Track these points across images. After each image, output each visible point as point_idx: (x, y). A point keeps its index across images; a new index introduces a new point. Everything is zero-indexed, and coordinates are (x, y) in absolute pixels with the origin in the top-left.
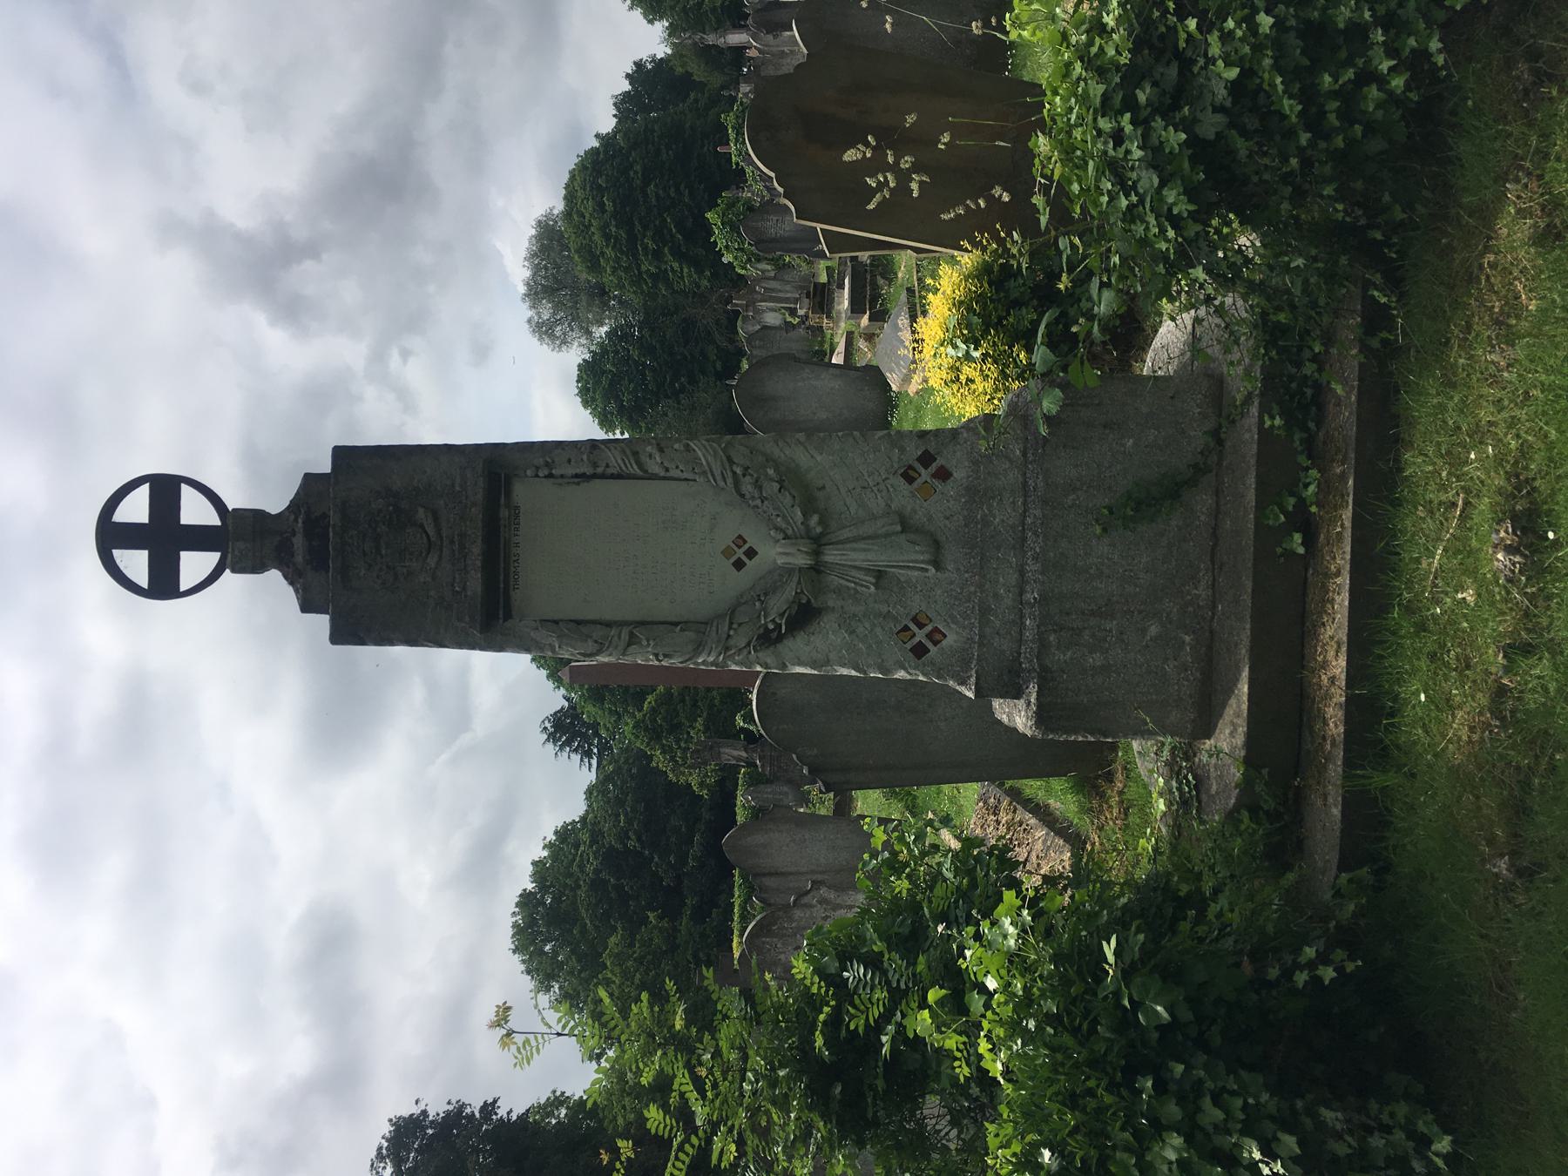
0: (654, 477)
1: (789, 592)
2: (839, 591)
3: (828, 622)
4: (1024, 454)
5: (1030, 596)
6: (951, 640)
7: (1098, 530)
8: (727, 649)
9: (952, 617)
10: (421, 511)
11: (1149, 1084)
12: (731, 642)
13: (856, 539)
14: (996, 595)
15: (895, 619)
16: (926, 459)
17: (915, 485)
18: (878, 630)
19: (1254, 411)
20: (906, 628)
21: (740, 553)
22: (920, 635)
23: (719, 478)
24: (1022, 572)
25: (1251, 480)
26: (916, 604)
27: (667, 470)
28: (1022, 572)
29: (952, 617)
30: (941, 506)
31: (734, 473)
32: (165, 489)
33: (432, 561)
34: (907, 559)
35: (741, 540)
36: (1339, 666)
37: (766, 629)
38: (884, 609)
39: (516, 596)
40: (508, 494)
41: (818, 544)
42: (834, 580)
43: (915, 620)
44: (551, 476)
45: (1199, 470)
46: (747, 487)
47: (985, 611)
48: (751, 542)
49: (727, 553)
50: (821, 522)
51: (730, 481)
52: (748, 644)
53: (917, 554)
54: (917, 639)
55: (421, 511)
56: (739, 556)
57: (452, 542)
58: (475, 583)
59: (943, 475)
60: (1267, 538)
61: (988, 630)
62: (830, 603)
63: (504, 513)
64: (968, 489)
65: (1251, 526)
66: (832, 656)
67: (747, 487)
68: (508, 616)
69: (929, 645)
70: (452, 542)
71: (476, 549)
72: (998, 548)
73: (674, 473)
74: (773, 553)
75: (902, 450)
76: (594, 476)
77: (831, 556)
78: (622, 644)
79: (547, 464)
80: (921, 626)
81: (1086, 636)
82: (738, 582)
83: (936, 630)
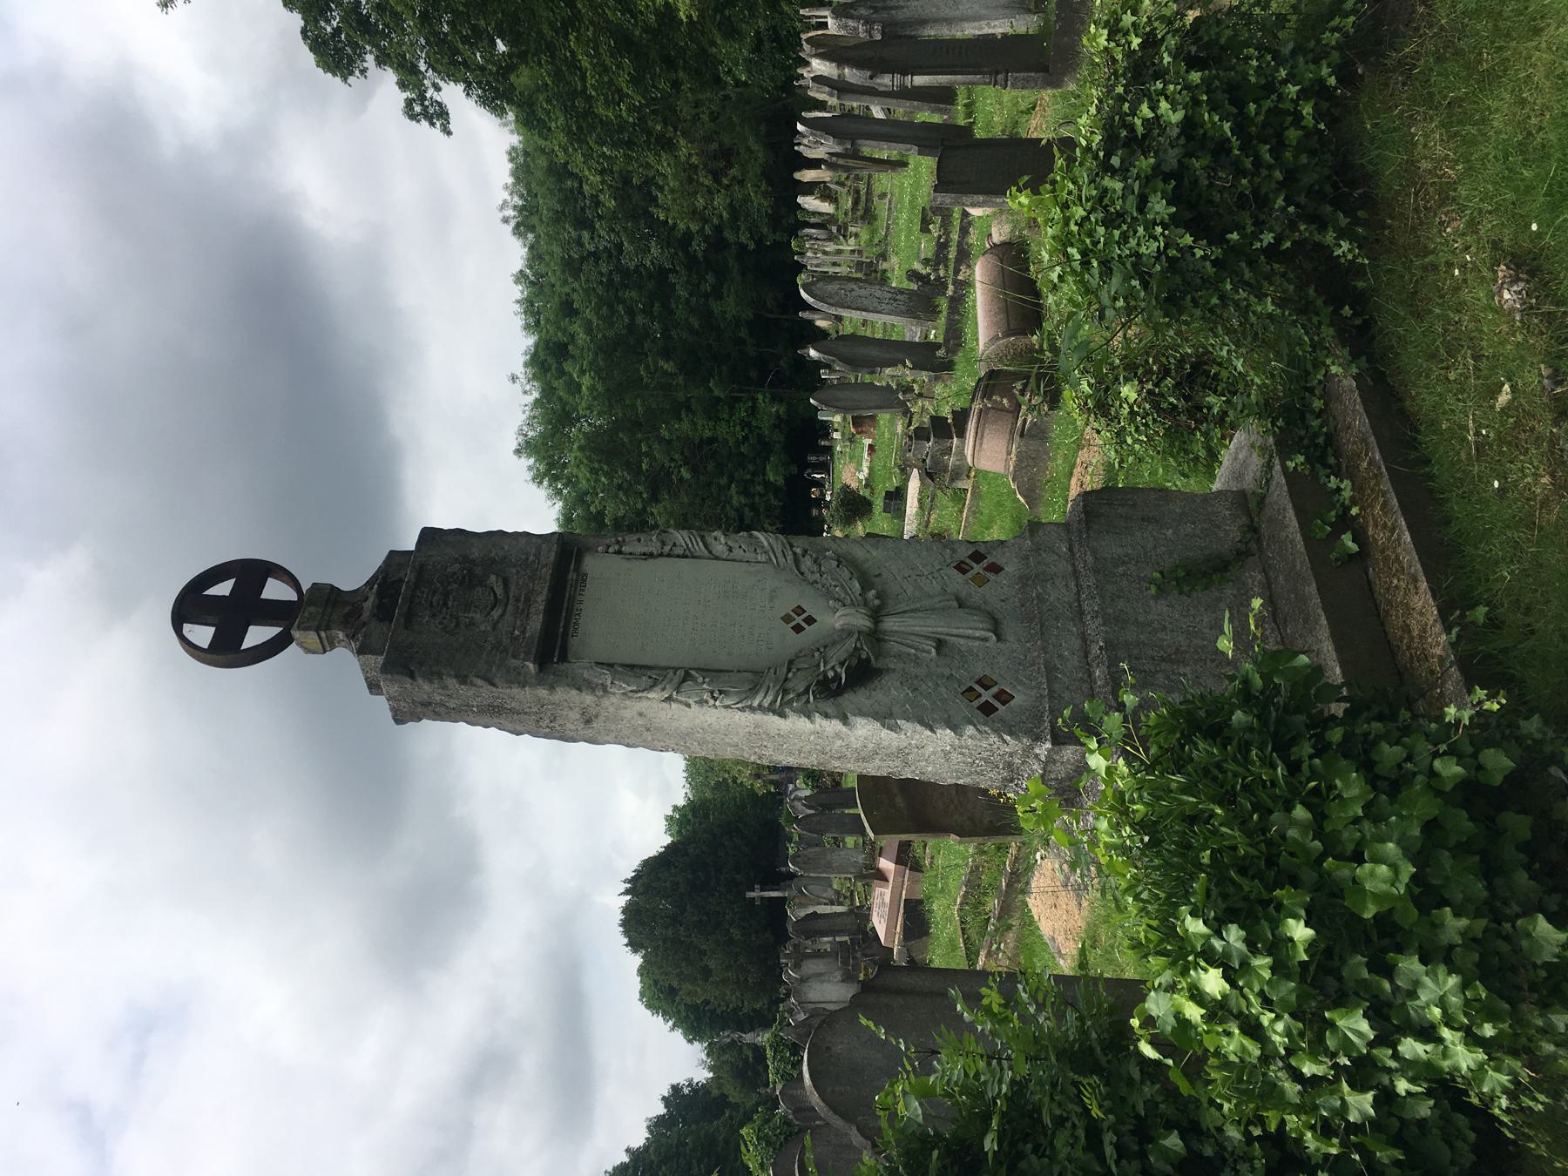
0: (717, 558)
1: (851, 644)
2: (899, 656)
3: (888, 680)
4: (1071, 549)
5: (1095, 650)
6: (1019, 700)
7: (1153, 590)
8: (785, 692)
9: (1017, 680)
10: (493, 578)
11: (1334, 1151)
12: (790, 685)
13: (912, 611)
14: (1060, 656)
15: (960, 682)
16: (977, 557)
17: (969, 575)
18: (943, 690)
19: (1277, 461)
20: (971, 689)
21: (799, 620)
22: (987, 696)
23: (780, 555)
24: (1084, 638)
25: (1291, 513)
26: (980, 670)
27: (730, 550)
28: (1084, 638)
29: (1017, 680)
30: (998, 591)
31: (795, 554)
32: (251, 573)
33: (496, 614)
34: (968, 631)
35: (799, 610)
36: (1423, 602)
37: (826, 676)
38: (947, 672)
39: (574, 642)
40: (579, 562)
41: (876, 615)
42: (893, 647)
43: (979, 682)
44: (619, 552)
45: (1242, 554)
46: (807, 563)
47: (1050, 670)
48: (810, 611)
49: (787, 619)
50: (878, 596)
51: (790, 557)
52: (807, 691)
53: (976, 628)
54: (983, 699)
55: (493, 578)
56: (799, 620)
57: (518, 600)
58: (536, 624)
59: (995, 569)
60: (1318, 548)
61: (1056, 686)
62: (892, 666)
63: (572, 576)
64: (1021, 578)
65: (1300, 545)
66: (895, 710)
67: (807, 563)
68: (564, 658)
69: (997, 704)
70: (518, 600)
71: (540, 601)
72: (1057, 619)
73: (738, 553)
74: (836, 619)
75: (954, 551)
76: (661, 555)
77: (890, 624)
78: (676, 680)
79: (618, 542)
80: (987, 688)
81: (1161, 678)
82: (795, 642)
83: (1003, 691)
